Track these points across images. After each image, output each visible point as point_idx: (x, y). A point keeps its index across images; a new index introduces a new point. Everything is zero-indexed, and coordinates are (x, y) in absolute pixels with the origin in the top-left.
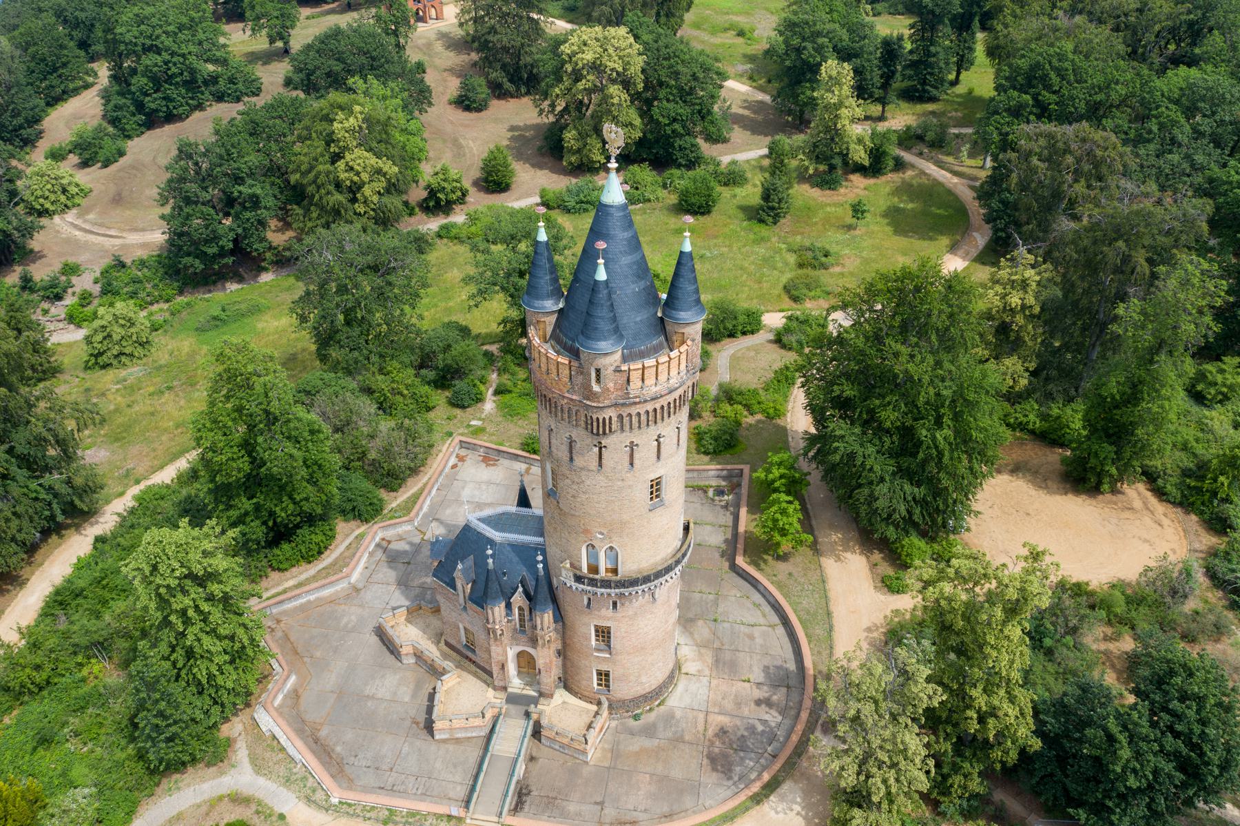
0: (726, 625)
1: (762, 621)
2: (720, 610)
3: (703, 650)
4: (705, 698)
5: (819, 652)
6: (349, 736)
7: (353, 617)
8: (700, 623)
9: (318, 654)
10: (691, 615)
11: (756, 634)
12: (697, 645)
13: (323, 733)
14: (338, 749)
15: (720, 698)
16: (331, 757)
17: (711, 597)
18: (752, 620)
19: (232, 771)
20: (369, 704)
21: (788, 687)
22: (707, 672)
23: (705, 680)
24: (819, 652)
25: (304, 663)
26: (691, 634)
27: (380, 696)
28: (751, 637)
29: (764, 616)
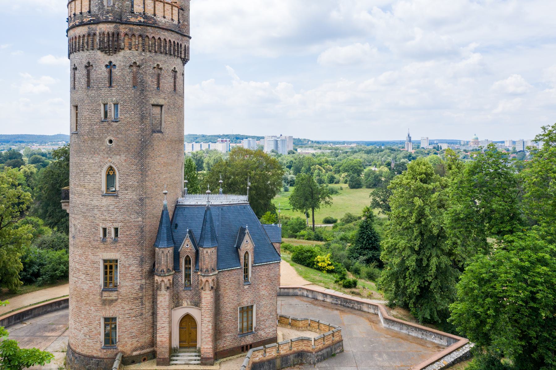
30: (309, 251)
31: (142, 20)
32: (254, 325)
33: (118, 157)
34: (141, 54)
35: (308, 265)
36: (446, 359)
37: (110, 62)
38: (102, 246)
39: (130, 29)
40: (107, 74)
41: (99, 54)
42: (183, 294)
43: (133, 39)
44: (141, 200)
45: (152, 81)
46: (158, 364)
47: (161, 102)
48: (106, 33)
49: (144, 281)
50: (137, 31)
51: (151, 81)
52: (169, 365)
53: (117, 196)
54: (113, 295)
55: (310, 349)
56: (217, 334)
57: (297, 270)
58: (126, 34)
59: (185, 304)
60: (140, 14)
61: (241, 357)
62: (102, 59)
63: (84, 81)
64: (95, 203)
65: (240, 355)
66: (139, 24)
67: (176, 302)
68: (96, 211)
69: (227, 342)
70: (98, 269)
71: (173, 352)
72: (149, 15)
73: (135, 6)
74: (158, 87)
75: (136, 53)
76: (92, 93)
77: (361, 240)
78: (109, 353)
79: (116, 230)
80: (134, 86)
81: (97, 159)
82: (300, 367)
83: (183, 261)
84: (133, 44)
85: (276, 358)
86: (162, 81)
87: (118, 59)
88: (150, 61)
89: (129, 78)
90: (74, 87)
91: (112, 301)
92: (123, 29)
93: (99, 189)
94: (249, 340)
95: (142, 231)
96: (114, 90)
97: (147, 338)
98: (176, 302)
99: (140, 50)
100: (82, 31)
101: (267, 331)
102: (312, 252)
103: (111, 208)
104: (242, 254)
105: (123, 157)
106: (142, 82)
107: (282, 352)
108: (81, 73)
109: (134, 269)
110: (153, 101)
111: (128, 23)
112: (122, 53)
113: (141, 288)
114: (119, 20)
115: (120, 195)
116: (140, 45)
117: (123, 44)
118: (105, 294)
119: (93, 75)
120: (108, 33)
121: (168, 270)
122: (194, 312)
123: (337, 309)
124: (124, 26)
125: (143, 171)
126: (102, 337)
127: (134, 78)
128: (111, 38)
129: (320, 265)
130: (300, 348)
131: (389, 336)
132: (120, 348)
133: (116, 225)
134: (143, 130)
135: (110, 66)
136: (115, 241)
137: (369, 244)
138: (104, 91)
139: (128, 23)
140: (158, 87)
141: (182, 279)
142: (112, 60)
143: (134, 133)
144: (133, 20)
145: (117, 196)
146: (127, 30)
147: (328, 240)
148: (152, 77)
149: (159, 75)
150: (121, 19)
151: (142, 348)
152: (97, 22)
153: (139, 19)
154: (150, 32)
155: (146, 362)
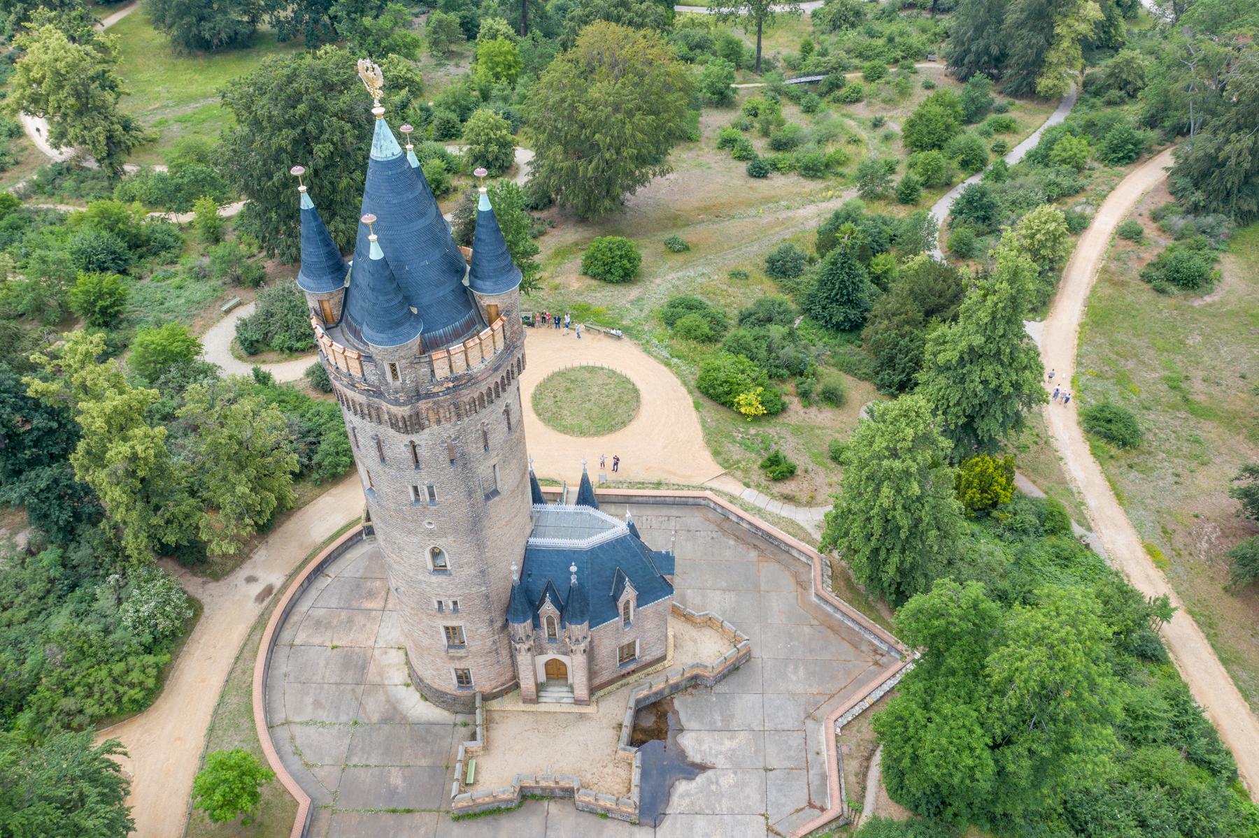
0: (343, 718)
1: (297, 730)
2: (347, 741)
3: (378, 680)
4: (383, 624)
5: (244, 672)
6: (728, 554)
7: (794, 678)
8: (375, 718)
9: (807, 629)
10: (386, 728)
11: (310, 709)
12: (383, 685)
13: (753, 554)
14: (732, 542)
15: (368, 625)
16: (734, 535)
17: (355, 760)
18: (311, 730)
19: (816, 523)
20: (724, 584)
21: (292, 646)
22: (377, 652)
23: (381, 643)
24: (244, 672)
25: (814, 618)
26: (388, 701)
27: (718, 593)
28: (317, 704)
29: (292, 738)
30: (726, 382)
31: (451, 385)
32: (637, 653)
33: (444, 539)
34: (456, 425)
35: (723, 404)
36: (873, 695)
37: (412, 442)
38: (439, 615)
39: (435, 403)
40: (411, 456)
41: (392, 432)
43: (441, 411)
44: (482, 572)
45: (477, 448)
46: (524, 702)
48: (400, 416)
49: (496, 637)
50: (445, 401)
51: (475, 449)
52: (538, 703)
53: (450, 574)
54: (462, 652)
55: (706, 674)
56: (592, 673)
57: (703, 423)
60: (447, 378)
61: (622, 686)
64: (420, 577)
65: (620, 683)
68: (424, 586)
69: (605, 676)
70: (438, 632)
71: (540, 687)
72: (460, 373)
73: (436, 371)
74: (486, 447)
75: (448, 425)
77: (829, 285)
78: (466, 692)
79: (455, 603)
80: (452, 461)
81: (415, 540)
82: (694, 691)
83: (544, 621)
84: (442, 415)
85: (664, 689)
86: (491, 437)
88: (471, 425)
89: (444, 457)
91: (460, 658)
92: (423, 405)
93: (425, 568)
94: (632, 667)
95: (487, 597)
96: (423, 473)
97: (509, 675)
99: (454, 419)
101: (653, 654)
102: (732, 384)
103: (444, 584)
104: (621, 605)
105: (451, 539)
106: (463, 455)
107: (671, 682)
109: (484, 629)
111: (429, 395)
112: (427, 431)
113: (494, 642)
114: (417, 395)
115: (453, 573)
116: (453, 414)
117: (427, 422)
118: (450, 650)
120: (403, 417)
121: (528, 637)
123: (755, 546)
124: (424, 401)
125: (480, 546)
126: (455, 680)
128: (408, 423)
129: (743, 410)
130: (694, 673)
131: (816, 622)
132: (477, 690)
133: (455, 599)
134: (473, 505)
136: (455, 610)
137: (842, 296)
139: (429, 395)
142: (413, 439)
143: (462, 511)
145: (450, 574)
146: (430, 405)
147: (779, 166)
148: (476, 443)
149: (485, 434)
150: (418, 394)
151: (503, 684)
152: (379, 394)
153: (445, 385)
155: (511, 694)
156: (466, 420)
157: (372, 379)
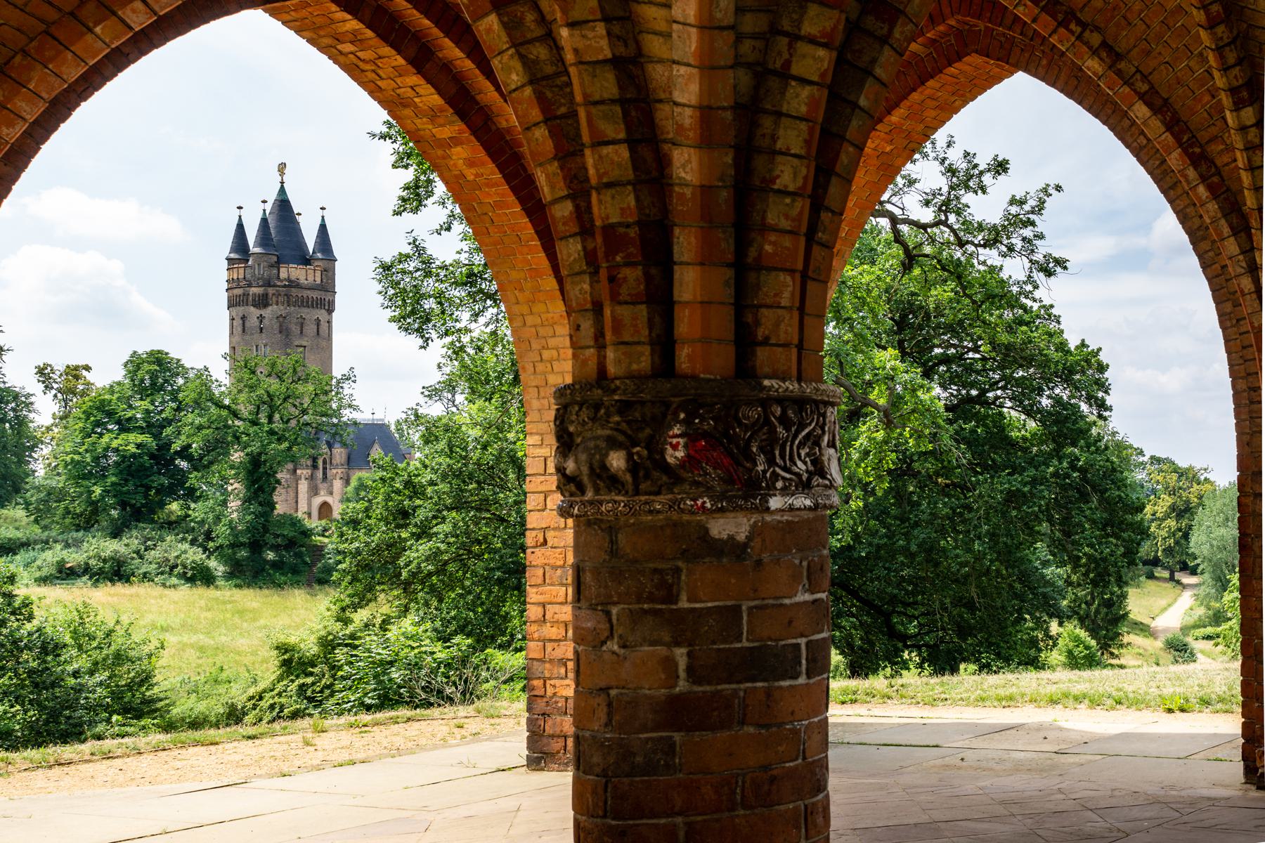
41: (252, 308)
42: (321, 486)
47: (304, 343)
51: (295, 329)
58: (273, 294)
59: (322, 493)
62: (254, 312)
63: (240, 329)
66: (285, 286)
67: (314, 491)
74: (301, 333)
76: (247, 337)
86: (305, 328)
87: (268, 312)
89: (276, 326)
90: (232, 333)
92: (271, 291)
96: (263, 335)
98: (314, 491)
100: (238, 292)
106: (287, 329)
108: (238, 322)
110: (297, 343)
111: (275, 286)
112: (270, 308)
114: (268, 284)
119: (248, 324)
122: (329, 499)
127: (281, 326)
135: (261, 318)
138: (257, 336)
139: (275, 286)
140: (301, 333)
141: (320, 474)
144: (279, 283)
152: (250, 286)
154: (294, 292)
156: (293, 308)
157: (248, 276)
